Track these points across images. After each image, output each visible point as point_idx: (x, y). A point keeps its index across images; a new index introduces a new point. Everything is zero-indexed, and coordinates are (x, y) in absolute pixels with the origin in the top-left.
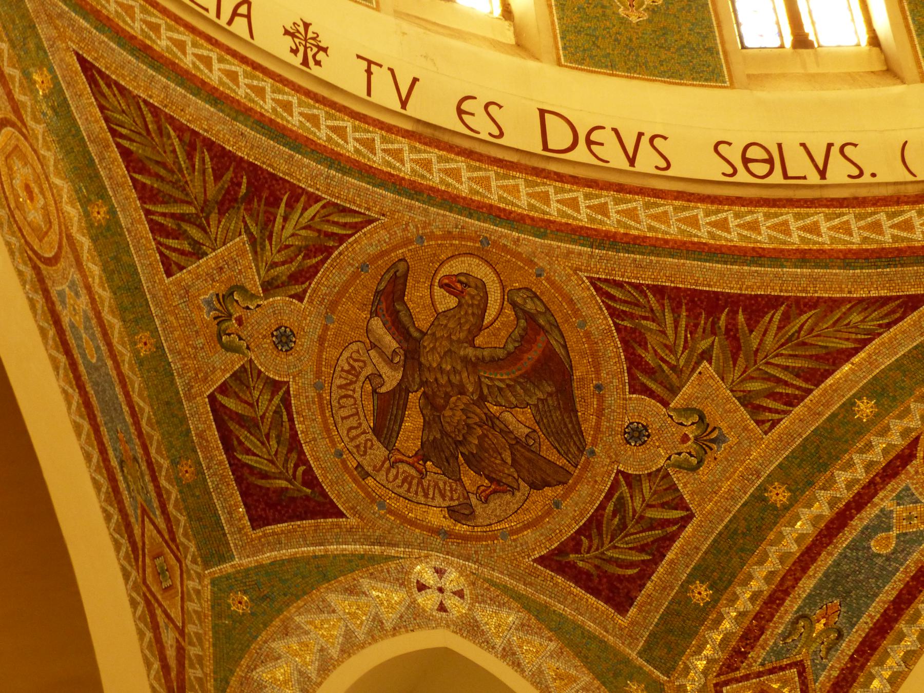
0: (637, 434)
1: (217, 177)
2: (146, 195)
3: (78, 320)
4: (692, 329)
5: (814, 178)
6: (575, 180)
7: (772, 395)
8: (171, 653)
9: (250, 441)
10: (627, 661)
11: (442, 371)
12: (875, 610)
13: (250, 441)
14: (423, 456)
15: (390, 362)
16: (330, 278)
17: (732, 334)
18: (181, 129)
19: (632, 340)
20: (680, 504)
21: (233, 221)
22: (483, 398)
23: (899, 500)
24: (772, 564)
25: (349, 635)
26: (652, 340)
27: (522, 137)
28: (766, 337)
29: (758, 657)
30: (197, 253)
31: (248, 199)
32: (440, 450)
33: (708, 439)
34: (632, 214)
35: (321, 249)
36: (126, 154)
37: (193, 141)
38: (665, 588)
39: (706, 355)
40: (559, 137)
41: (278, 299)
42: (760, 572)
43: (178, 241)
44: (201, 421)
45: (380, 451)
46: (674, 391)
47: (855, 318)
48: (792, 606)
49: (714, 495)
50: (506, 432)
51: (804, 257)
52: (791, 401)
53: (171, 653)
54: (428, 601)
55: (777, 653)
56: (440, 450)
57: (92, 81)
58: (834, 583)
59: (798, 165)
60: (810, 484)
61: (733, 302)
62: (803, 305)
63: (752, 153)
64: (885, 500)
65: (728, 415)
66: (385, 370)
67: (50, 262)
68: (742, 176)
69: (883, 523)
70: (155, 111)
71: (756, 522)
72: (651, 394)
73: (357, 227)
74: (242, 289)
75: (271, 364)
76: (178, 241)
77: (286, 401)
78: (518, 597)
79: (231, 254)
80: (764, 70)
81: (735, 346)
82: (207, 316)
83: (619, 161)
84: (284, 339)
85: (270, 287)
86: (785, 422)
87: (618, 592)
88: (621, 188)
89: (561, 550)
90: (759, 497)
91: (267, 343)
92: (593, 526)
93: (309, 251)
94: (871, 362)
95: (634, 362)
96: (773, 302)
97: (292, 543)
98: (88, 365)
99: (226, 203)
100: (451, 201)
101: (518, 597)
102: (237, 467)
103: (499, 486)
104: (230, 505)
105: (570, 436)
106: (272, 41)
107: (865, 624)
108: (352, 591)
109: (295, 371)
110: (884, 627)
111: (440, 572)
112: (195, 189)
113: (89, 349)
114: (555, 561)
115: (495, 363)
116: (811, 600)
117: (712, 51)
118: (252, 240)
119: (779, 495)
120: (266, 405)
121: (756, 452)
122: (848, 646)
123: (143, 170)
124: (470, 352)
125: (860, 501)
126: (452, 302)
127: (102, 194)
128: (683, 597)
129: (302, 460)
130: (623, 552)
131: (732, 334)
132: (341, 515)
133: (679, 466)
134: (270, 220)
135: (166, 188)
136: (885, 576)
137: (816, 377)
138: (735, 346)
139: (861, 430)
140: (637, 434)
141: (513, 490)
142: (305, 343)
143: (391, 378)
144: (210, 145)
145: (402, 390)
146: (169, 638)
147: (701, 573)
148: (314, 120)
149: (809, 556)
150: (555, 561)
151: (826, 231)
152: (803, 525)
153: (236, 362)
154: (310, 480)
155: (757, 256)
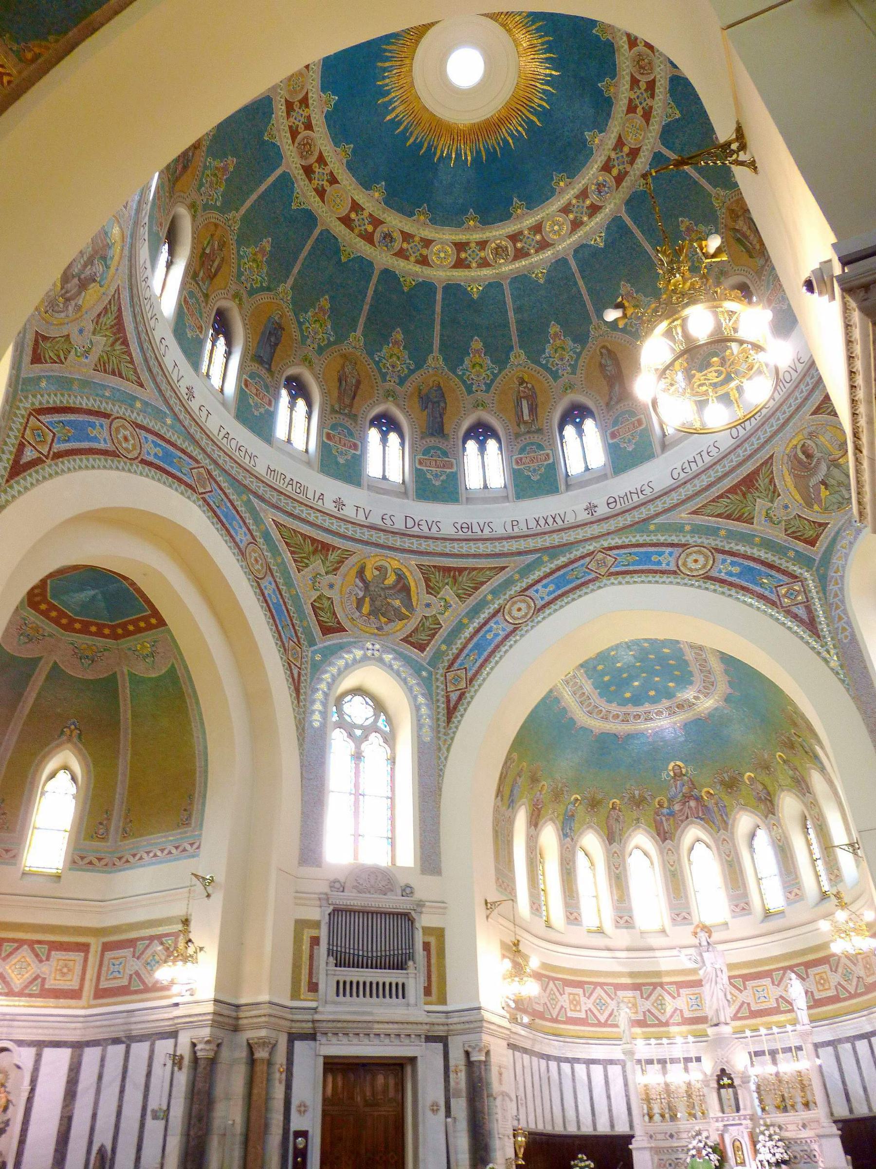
0: (428, 605)
2: (292, 553)
3: (271, 592)
4: (444, 577)
5: (480, 532)
6: (413, 536)
7: (465, 594)
8: (296, 675)
9: (322, 614)
10: (422, 666)
12: (486, 654)
13: (322, 614)
15: (361, 590)
16: (343, 569)
17: (454, 578)
18: (302, 534)
19: (427, 580)
20: (439, 624)
21: (317, 557)
23: (495, 623)
24: (463, 640)
25: (347, 663)
26: (433, 580)
27: (399, 525)
28: (463, 578)
29: (456, 665)
30: (307, 566)
31: (321, 551)
32: (375, 612)
33: (447, 606)
34: (428, 545)
35: (341, 562)
36: (286, 543)
38: (434, 646)
39: (447, 584)
40: (410, 523)
41: (330, 576)
42: (459, 642)
43: (301, 564)
44: (308, 610)
46: (438, 593)
47: (488, 572)
48: (466, 651)
49: (448, 621)
50: (393, 606)
51: (474, 556)
52: (470, 595)
53: (296, 675)
54: (369, 653)
55: (461, 665)
56: (375, 612)
57: (277, 526)
58: (477, 646)
59: (476, 529)
60: (473, 618)
61: (455, 569)
62: (474, 569)
63: (465, 526)
64: (492, 623)
65: (453, 600)
66: (359, 592)
67: (261, 579)
68: (460, 533)
69: (490, 631)
70: (294, 530)
71: (459, 627)
72: (431, 594)
73: (351, 555)
75: (328, 593)
76: (301, 564)
77: (332, 603)
78: (394, 650)
79: (317, 564)
80: (471, 499)
81: (455, 579)
82: (310, 582)
83: (426, 529)
84: (331, 586)
85: (327, 573)
86: (468, 601)
87: (422, 648)
88: (426, 538)
89: (407, 637)
90: (460, 621)
91: (327, 588)
92: (416, 630)
94: (491, 584)
95: (428, 586)
96: (465, 569)
97: (334, 640)
98: (273, 604)
99: (315, 552)
100: (377, 545)
101: (394, 650)
102: (318, 620)
103: (390, 621)
104: (316, 631)
105: (409, 606)
106: (329, 506)
107: (483, 657)
108: (349, 652)
109: (333, 594)
110: (486, 660)
111: (373, 645)
112: (306, 550)
113: (274, 599)
114: (405, 640)
115: (389, 588)
116: (471, 650)
117: (458, 493)
119: (465, 621)
120: (326, 603)
121: (459, 608)
122: (478, 664)
124: (382, 586)
125: (485, 624)
126: (378, 573)
127: (280, 554)
128: (439, 649)
129: (336, 617)
130: (423, 637)
131: (454, 578)
133: (439, 613)
136: (490, 644)
137: (476, 589)
138: (455, 579)
139: (488, 603)
140: (428, 605)
141: (394, 621)
142: (337, 587)
143: (361, 594)
144: (310, 537)
145: (364, 597)
146: (295, 672)
147: (444, 642)
148: (340, 526)
149: (471, 638)
150: (405, 640)
151: (482, 548)
152: (471, 629)
153: (318, 593)
154: (339, 623)
155: (462, 556)
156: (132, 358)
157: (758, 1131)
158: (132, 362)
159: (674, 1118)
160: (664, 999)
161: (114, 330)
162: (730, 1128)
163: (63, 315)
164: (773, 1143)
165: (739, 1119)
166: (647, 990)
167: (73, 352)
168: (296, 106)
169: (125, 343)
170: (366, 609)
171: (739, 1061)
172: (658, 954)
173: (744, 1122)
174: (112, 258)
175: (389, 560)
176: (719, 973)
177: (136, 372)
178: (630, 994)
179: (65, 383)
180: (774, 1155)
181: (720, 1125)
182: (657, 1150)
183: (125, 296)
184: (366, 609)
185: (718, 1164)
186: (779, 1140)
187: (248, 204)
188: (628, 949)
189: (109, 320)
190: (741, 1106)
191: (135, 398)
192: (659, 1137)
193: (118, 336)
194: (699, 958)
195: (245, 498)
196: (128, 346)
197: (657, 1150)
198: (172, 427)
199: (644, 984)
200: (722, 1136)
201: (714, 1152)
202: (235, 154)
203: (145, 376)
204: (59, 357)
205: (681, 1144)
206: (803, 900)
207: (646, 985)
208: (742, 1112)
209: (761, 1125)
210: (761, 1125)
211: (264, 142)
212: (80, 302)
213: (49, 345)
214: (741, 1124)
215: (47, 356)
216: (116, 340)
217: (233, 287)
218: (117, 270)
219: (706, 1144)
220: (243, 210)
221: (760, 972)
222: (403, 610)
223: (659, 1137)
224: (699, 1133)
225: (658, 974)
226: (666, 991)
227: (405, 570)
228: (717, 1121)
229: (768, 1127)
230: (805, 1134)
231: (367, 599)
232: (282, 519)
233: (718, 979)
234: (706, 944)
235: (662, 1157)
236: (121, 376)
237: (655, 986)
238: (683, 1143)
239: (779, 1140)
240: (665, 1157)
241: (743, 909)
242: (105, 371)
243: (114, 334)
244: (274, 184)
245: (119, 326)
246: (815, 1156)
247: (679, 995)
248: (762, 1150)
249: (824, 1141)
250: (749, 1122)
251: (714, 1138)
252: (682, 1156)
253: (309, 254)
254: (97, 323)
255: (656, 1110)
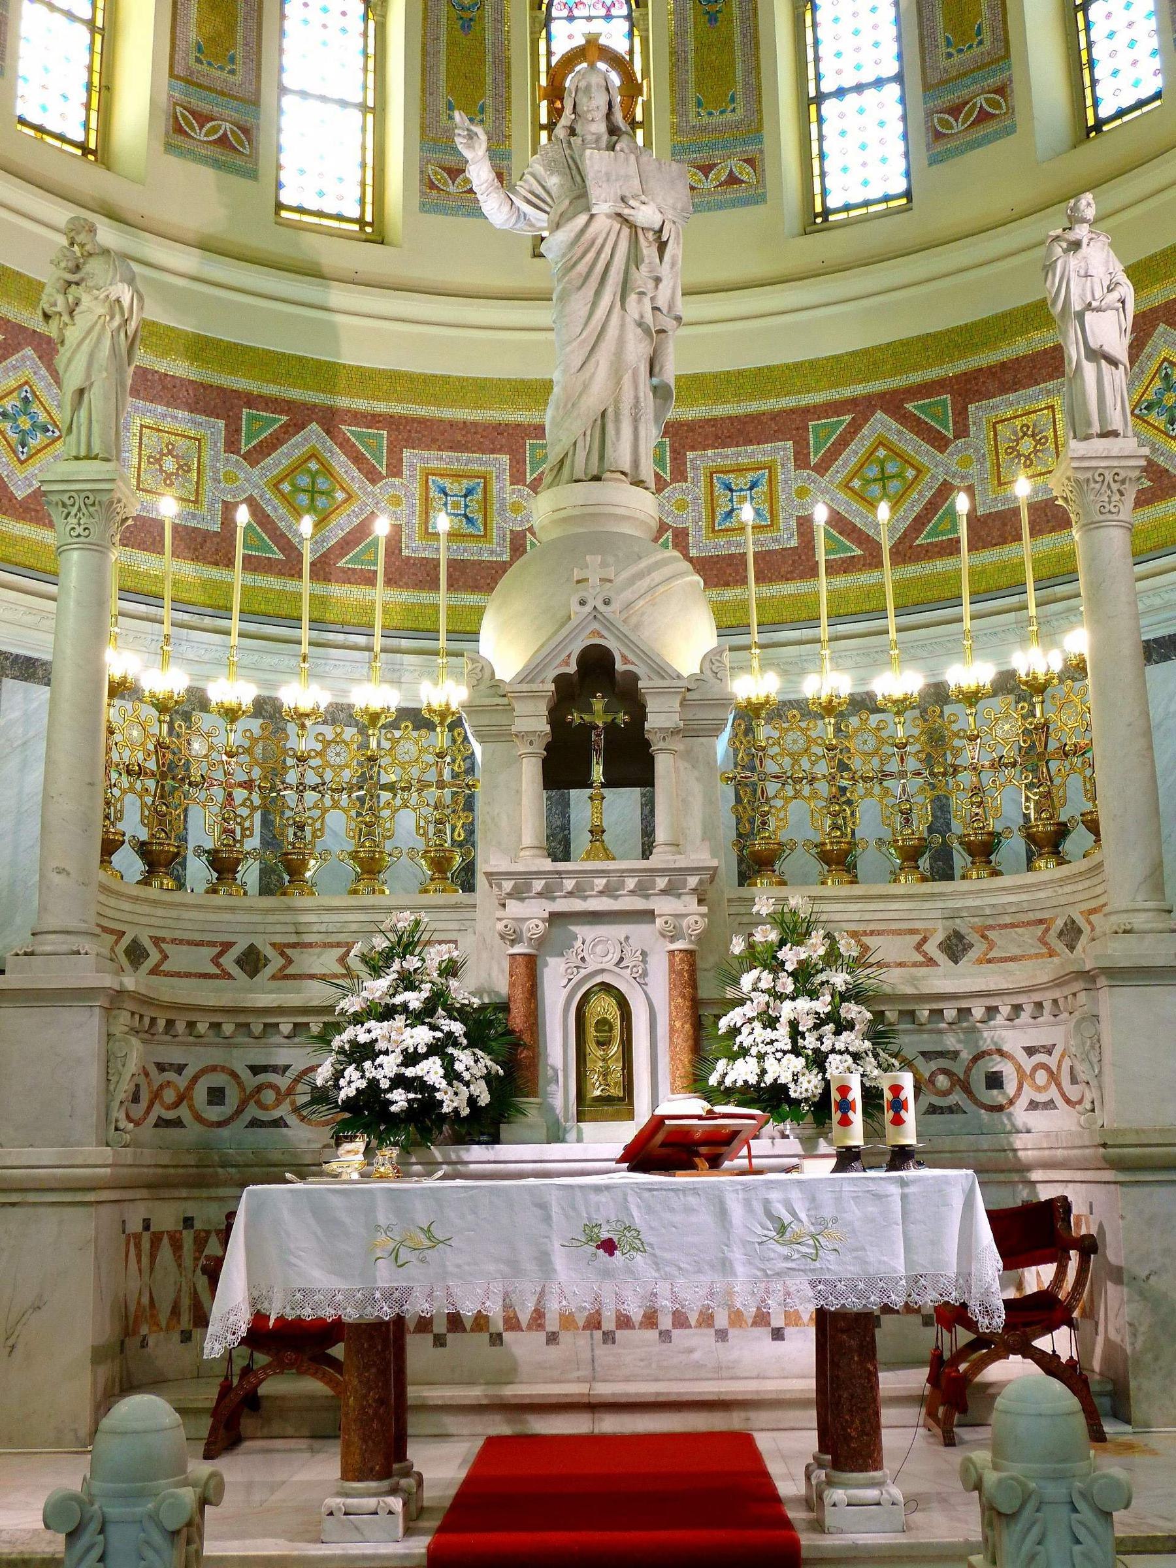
157: (738, 946)
159: (285, 871)
160: (327, 470)
162: (583, 932)
164: (822, 1005)
165: (642, 891)
166: (257, 425)
171: (681, 636)
172: (338, 296)
173: (663, 906)
176: (649, 251)
178: (180, 420)
180: (818, 1061)
181: (532, 913)
182: (155, 1020)
185: (484, 1099)
186: (853, 994)
188: (207, 246)
190: (661, 834)
192: (180, 958)
194: (553, 181)
197: (155, 1020)
199: (251, 400)
200: (529, 969)
201: (476, 1040)
205: (293, 999)
206: (1009, 131)
207: (262, 405)
208: (658, 859)
209: (759, 921)
210: (759, 921)
214: (648, 916)
219: (437, 1001)
221: (755, 419)
223: (180, 958)
224: (406, 945)
225: (326, 373)
226: (345, 445)
228: (518, 894)
229: (794, 930)
230: (947, 979)
233: (641, 277)
234: (601, 127)
235: (175, 1055)
237: (299, 416)
238: (316, 993)
239: (853, 994)
240: (195, 1059)
241: (733, 180)
246: (995, 1081)
247: (395, 470)
248: (754, 1036)
249: (1114, 1003)
250: (690, 905)
251: (485, 978)
252: (293, 1056)
255: (202, 829)
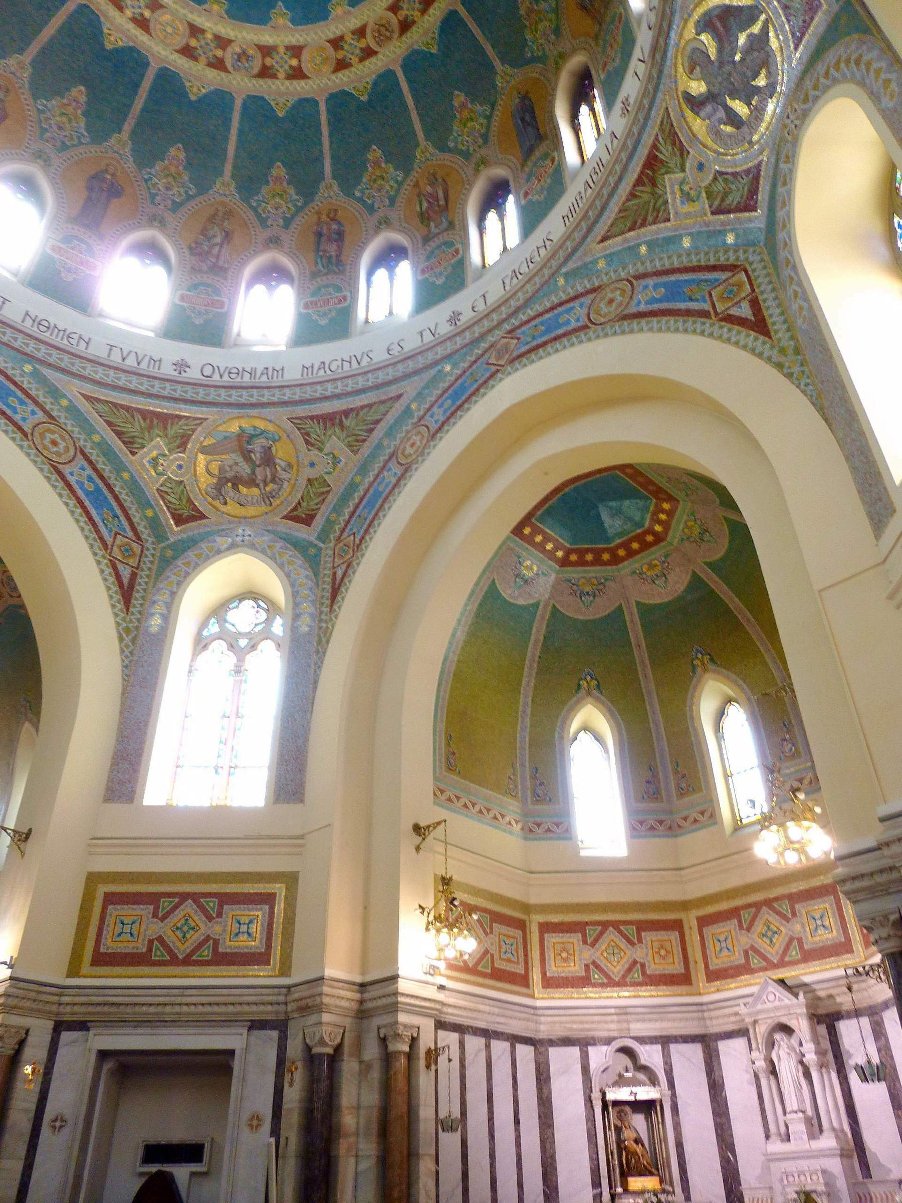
1: (644, 185)
2: (643, 225)
11: (720, 83)
14: (749, 104)
18: (628, 200)
22: (734, 62)
30: (666, 202)
32: (748, 94)
36: (631, 229)
37: (632, 195)
41: (688, 165)
43: (660, 214)
45: (745, 129)
70: (620, 211)
74: (682, 183)
76: (660, 214)
77: (721, 173)
85: (683, 170)
93: (674, 144)
112: (646, 197)
115: (720, 51)
118: (667, 172)
120: (720, 186)
123: (635, 222)
124: (716, 64)
126: (698, 68)
132: (760, 164)
134: (662, 162)
135: (643, 213)
143: (721, 114)
156: (366, 406)
158: (370, 406)
161: (329, 425)
163: (286, 484)
167: (326, 477)
168: (340, 55)
169: (347, 413)
170: (740, 108)
174: (255, 428)
175: (683, 42)
177: (382, 402)
179: (352, 487)
183: (301, 411)
184: (740, 108)
187: (417, 126)
189: (316, 429)
191: (408, 408)
193: (337, 421)
195: (561, 281)
196: (352, 410)
198: (455, 365)
202: (367, 148)
203: (393, 391)
204: (323, 493)
211: (370, 101)
212: (283, 464)
213: (304, 504)
215: (314, 507)
216: (341, 425)
217: (470, 170)
218: (270, 421)
220: (420, 135)
222: (756, 29)
227: (696, 16)
231: (729, 102)
232: (601, 228)
236: (378, 422)
242: (364, 441)
243: (333, 425)
244: (410, 81)
245: (328, 420)
253: (480, 25)
254: (312, 445)
